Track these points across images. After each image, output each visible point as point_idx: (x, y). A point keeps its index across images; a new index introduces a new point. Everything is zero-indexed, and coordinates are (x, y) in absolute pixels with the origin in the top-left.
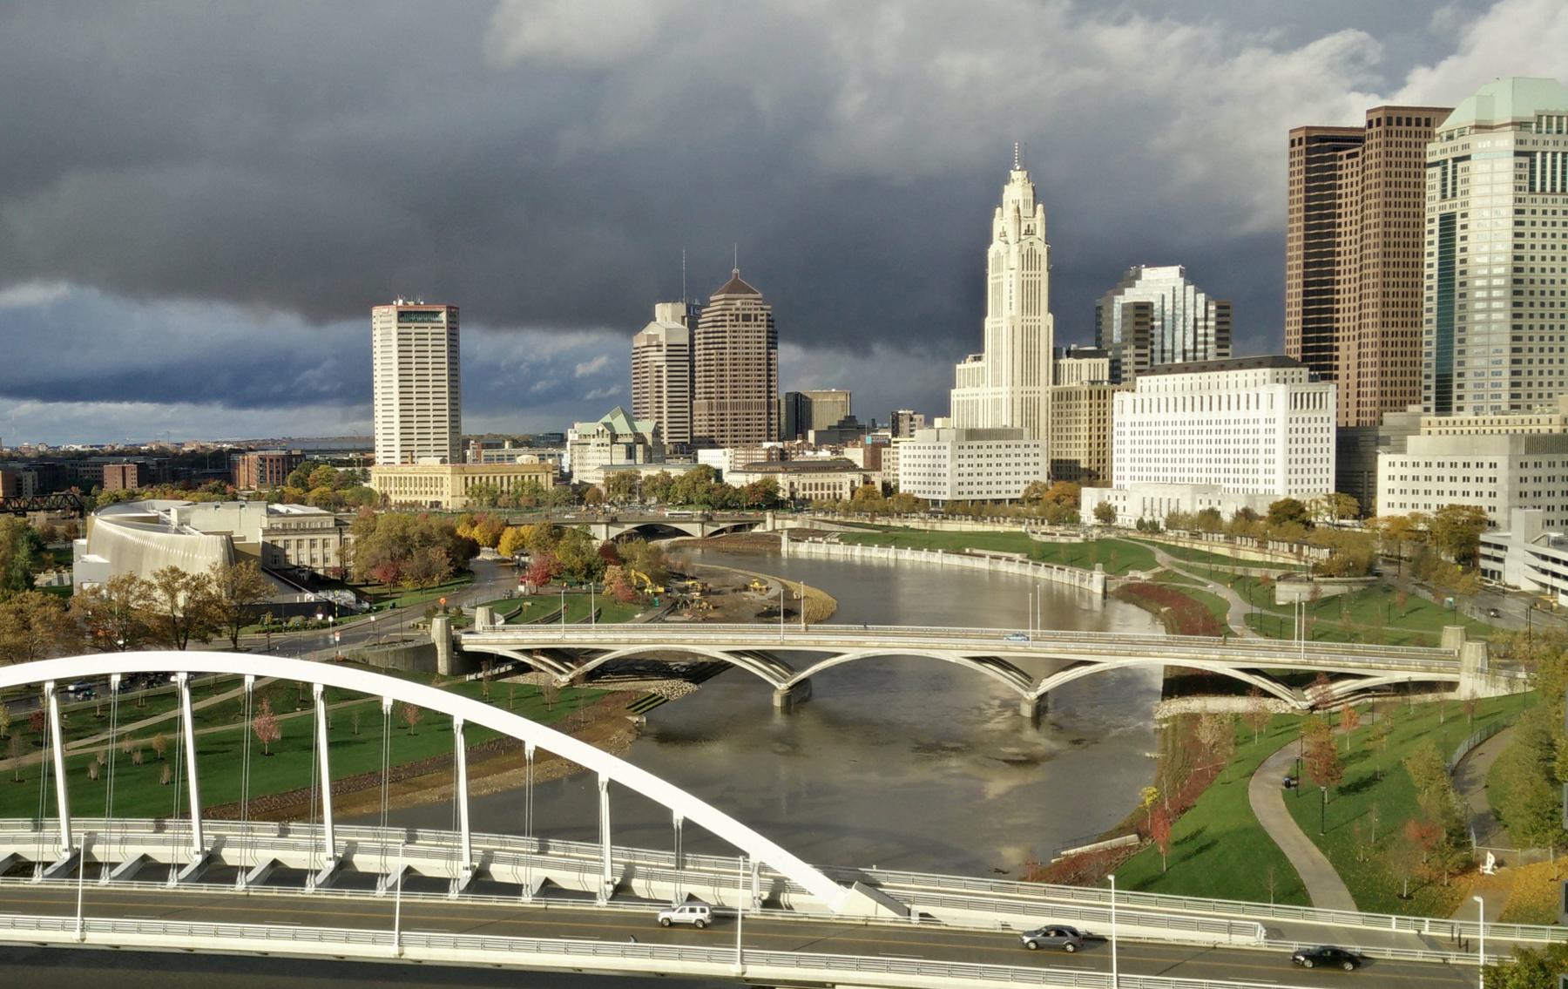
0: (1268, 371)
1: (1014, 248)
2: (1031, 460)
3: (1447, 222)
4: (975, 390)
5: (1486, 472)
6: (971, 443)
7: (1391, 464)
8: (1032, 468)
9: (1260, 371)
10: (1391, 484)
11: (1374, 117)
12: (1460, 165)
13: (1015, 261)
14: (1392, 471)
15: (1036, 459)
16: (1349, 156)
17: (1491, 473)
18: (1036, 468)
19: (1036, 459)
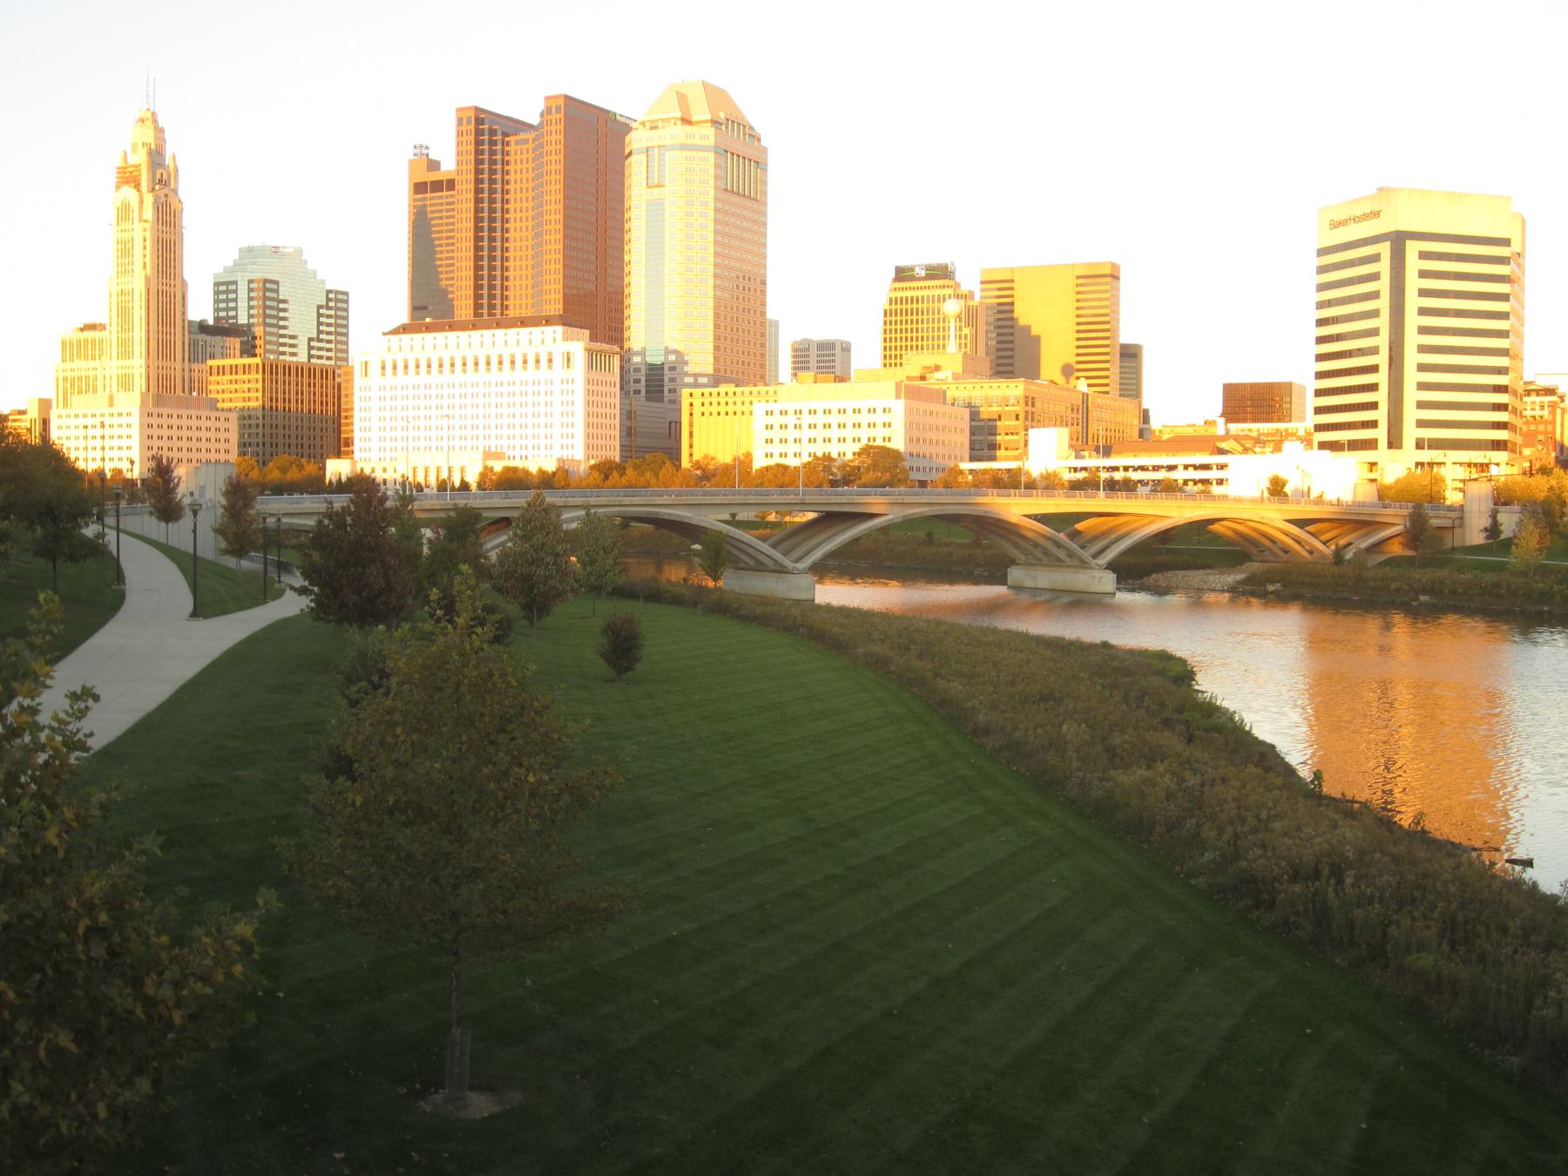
0: (559, 329)
1: (149, 199)
2: (222, 435)
3: (656, 208)
4: (91, 364)
5: (880, 418)
6: (160, 410)
7: (769, 413)
8: (222, 446)
9: (549, 330)
10: (769, 434)
11: (553, 104)
12: (668, 155)
13: (149, 213)
14: (769, 420)
15: (227, 435)
16: (517, 142)
17: (886, 418)
18: (226, 446)
19: (227, 435)
